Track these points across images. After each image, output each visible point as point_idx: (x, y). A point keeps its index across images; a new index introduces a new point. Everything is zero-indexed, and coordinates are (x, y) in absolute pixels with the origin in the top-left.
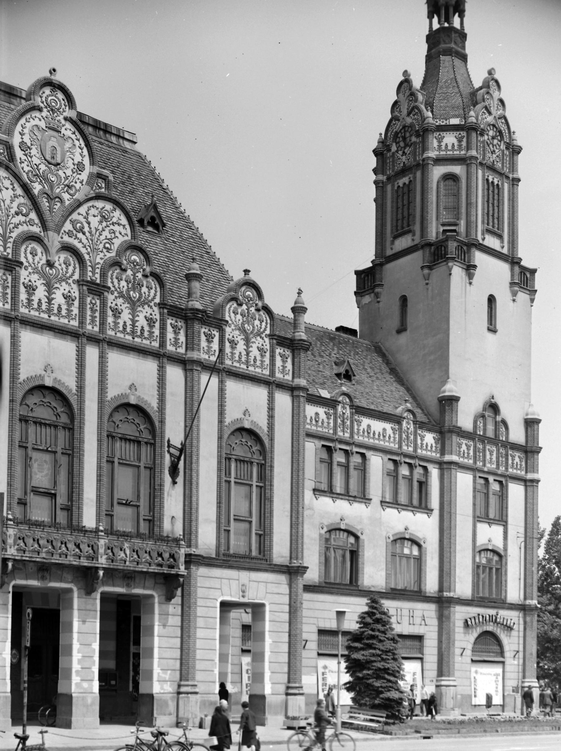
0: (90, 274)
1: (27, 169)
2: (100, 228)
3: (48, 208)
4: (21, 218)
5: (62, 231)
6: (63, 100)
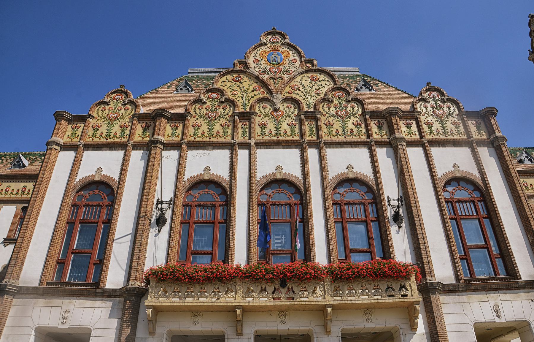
2: (311, 85)
4: (255, 92)
5: (284, 92)
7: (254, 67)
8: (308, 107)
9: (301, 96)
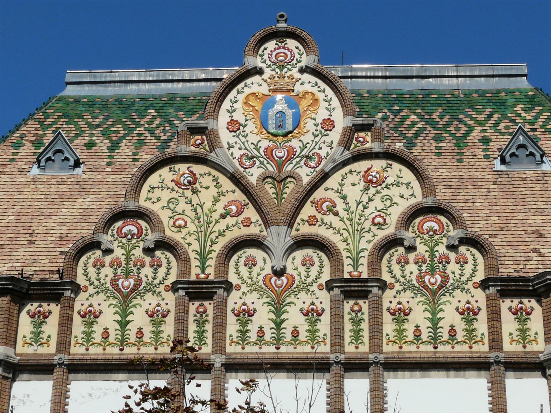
0: (350, 269)
1: (237, 153)
2: (365, 199)
3: (274, 196)
4: (230, 221)
5: (298, 220)
6: (297, 48)
7: (228, 143)
8: (356, 264)
9: (339, 232)
